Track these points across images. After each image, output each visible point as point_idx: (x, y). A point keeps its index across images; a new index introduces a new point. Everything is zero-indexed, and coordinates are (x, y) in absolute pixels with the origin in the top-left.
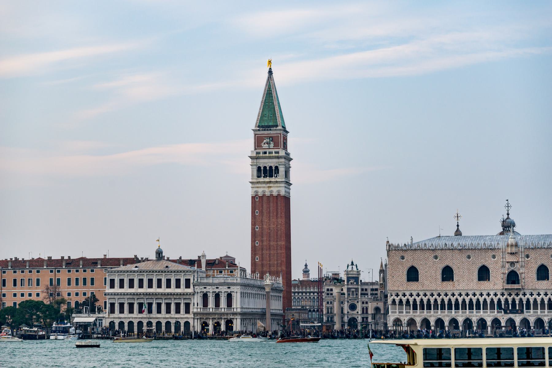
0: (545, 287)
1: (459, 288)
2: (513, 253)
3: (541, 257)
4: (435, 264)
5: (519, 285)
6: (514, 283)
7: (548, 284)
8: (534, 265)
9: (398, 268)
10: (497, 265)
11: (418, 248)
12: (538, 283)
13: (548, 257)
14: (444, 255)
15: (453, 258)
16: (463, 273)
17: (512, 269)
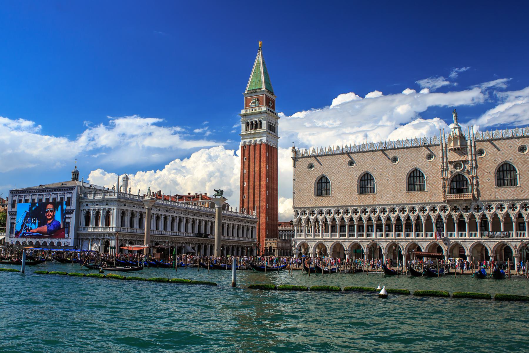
0: (511, 196)
1: (382, 201)
2: (458, 148)
3: (503, 152)
4: (350, 171)
5: (468, 195)
6: (460, 191)
7: (516, 191)
8: (491, 165)
9: (306, 179)
10: (434, 168)
11: (330, 153)
12: (500, 190)
13: (514, 150)
14: (362, 159)
15: (374, 162)
16: (387, 182)
17: (458, 172)
